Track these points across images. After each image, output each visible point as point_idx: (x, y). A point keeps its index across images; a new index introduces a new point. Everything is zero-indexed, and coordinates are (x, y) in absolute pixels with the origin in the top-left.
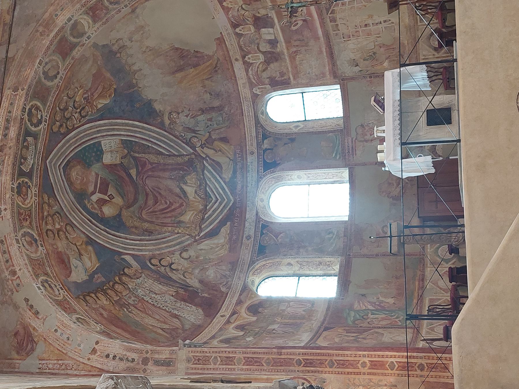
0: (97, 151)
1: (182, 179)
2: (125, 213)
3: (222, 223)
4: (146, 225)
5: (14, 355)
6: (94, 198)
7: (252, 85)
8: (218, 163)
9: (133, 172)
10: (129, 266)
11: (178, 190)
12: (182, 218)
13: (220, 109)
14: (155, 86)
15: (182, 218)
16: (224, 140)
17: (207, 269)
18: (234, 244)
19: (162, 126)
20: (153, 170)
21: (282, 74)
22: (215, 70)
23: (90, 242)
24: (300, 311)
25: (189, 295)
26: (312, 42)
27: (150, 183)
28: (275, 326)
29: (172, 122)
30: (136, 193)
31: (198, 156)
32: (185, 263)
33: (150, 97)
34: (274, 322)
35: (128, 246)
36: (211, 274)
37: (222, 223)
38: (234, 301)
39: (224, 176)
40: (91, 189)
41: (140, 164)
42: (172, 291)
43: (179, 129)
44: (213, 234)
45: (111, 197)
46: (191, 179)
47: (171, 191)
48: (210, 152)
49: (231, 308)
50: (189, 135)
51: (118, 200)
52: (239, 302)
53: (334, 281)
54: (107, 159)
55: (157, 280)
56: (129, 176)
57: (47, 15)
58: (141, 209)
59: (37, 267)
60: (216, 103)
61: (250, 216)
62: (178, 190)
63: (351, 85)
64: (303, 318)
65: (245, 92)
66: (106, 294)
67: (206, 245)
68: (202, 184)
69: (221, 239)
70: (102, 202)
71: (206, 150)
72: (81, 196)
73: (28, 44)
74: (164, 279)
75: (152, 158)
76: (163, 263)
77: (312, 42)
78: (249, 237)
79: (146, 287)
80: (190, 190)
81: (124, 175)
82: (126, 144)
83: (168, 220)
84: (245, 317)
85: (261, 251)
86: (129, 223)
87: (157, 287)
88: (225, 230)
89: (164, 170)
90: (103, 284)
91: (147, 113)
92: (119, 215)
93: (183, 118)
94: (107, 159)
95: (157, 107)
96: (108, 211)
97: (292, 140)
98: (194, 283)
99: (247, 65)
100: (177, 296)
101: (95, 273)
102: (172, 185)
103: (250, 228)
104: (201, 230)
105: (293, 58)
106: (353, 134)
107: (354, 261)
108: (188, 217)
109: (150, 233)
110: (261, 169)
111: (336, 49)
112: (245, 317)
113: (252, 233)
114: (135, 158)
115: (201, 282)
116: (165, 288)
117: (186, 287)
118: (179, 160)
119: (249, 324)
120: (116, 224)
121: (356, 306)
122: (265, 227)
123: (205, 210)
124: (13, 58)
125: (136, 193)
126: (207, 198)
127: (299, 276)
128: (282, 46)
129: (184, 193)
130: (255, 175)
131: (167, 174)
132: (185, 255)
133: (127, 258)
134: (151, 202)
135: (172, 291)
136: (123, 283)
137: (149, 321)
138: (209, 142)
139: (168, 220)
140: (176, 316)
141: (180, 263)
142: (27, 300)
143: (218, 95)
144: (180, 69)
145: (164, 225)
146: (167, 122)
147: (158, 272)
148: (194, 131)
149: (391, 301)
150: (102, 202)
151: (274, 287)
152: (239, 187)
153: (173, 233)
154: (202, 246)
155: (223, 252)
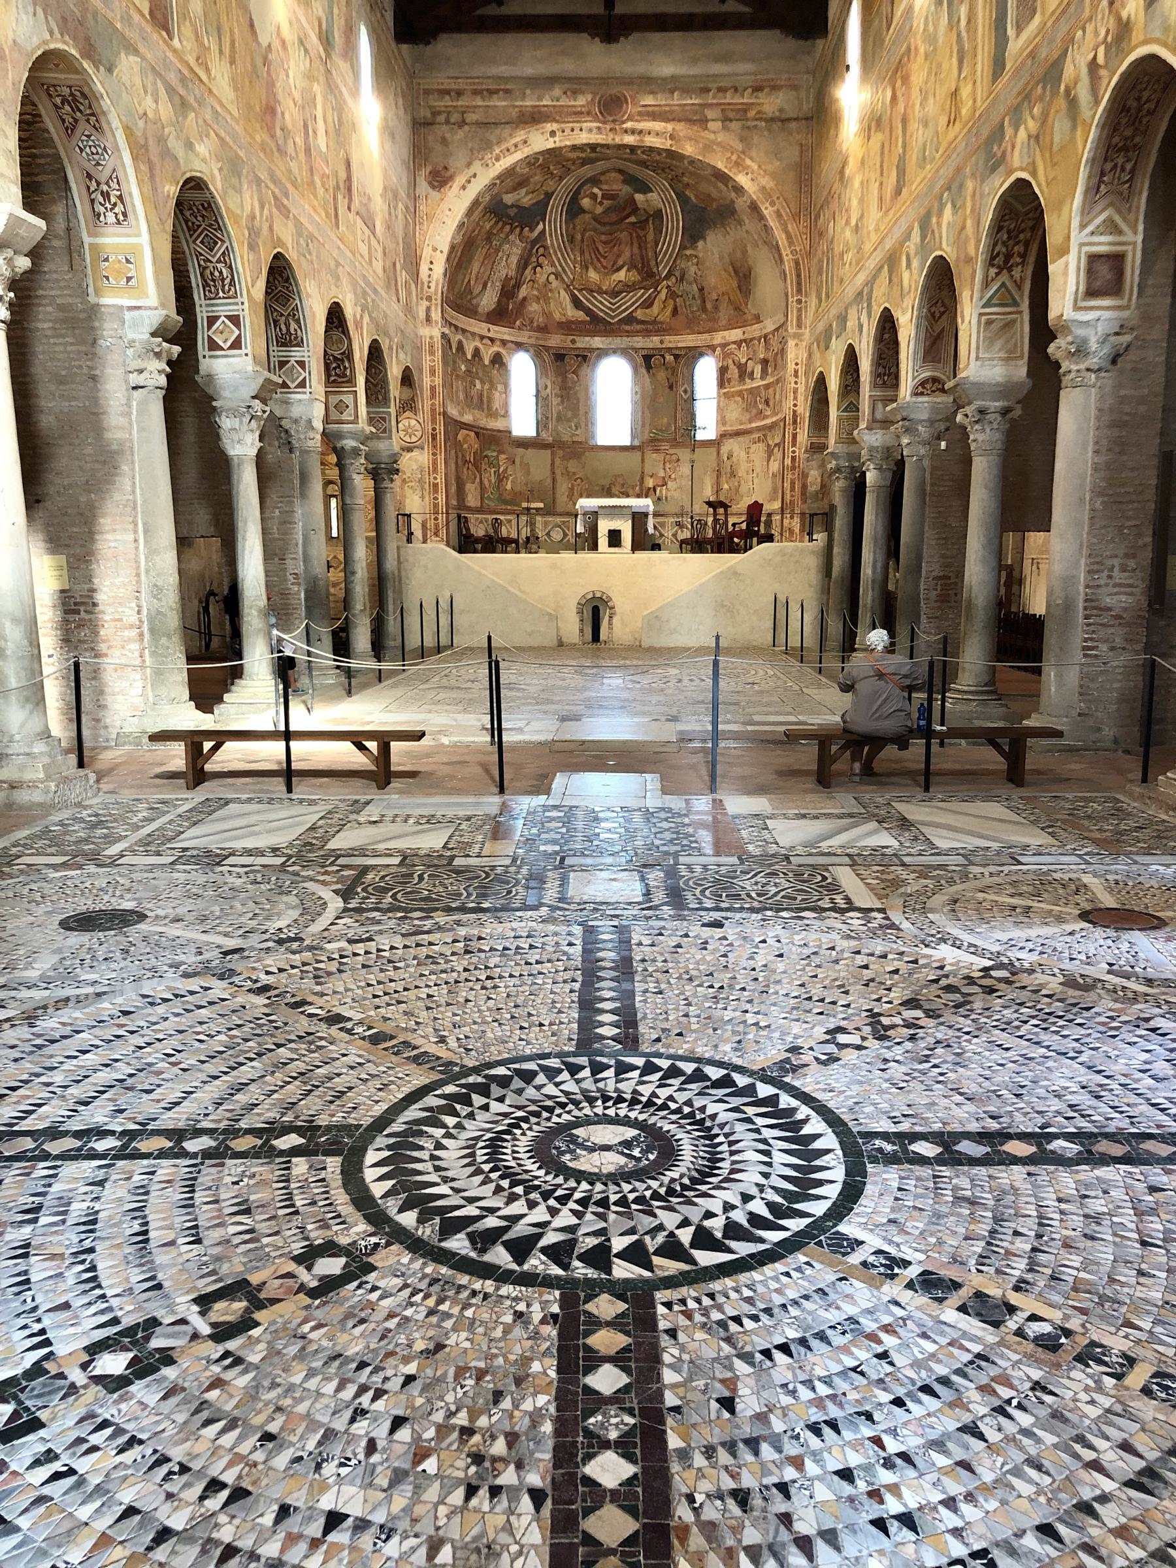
0: (645, 189)
1: (632, 266)
2: (587, 216)
3: (588, 312)
4: (579, 237)
5: (429, 168)
6: (596, 190)
7: (724, 346)
8: (652, 304)
9: (633, 219)
10: (532, 230)
11: (620, 262)
12: (591, 270)
13: (704, 309)
14: (715, 247)
15: (591, 270)
16: (675, 312)
17: (538, 302)
18: (568, 327)
19: (683, 247)
20: (638, 236)
21: (729, 380)
22: (737, 309)
23: (549, 196)
24: (496, 405)
25: (509, 291)
26: (748, 416)
27: (624, 236)
28: (478, 386)
29: (689, 258)
30: (611, 224)
31: (658, 283)
32: (543, 279)
33: (709, 239)
34: (483, 383)
35: (553, 227)
36: (534, 307)
37: (588, 312)
38: (506, 337)
39: (639, 311)
40: (605, 187)
41: (642, 225)
42: (512, 273)
43: (682, 264)
44: (577, 303)
45: (601, 203)
46: (634, 276)
47: (619, 256)
48: (663, 295)
49: (499, 336)
50: (677, 274)
51: (599, 210)
52: (504, 343)
53: (531, 432)
54: (639, 197)
55: (522, 256)
56: (627, 216)
57: (748, 162)
58: (595, 230)
59: (510, 172)
60: (709, 306)
61: (597, 342)
62: (620, 262)
63: (713, 450)
64: (489, 408)
65: (718, 338)
66: (497, 223)
67: (565, 297)
68: (629, 287)
69: (572, 313)
70: (593, 197)
71: (665, 291)
72: (594, 181)
73: (719, 144)
74: (523, 264)
75: (651, 236)
76: (541, 259)
77: (748, 416)
78: (573, 342)
79: (513, 251)
80: (622, 275)
81: (628, 211)
82: (658, 214)
83: (587, 255)
84: (487, 354)
85: (560, 357)
86: (577, 221)
87: (514, 260)
88: (581, 315)
89: (640, 247)
90: (508, 216)
91: (694, 233)
92: (584, 211)
93: (693, 269)
94: (639, 197)
95: (700, 244)
96: (586, 202)
97: (671, 387)
98: (523, 292)
99: (739, 343)
100: (507, 279)
101: (518, 207)
102: (626, 255)
103: (583, 342)
104: (580, 290)
105: (740, 393)
106: (672, 451)
107: (549, 452)
108: (593, 275)
109: (572, 240)
110: (644, 352)
111: (740, 439)
112: (487, 354)
113: (578, 345)
114: (647, 220)
115: (525, 299)
116: (514, 266)
117: (518, 285)
118: (653, 263)
119: (481, 359)
120: (574, 210)
121: (503, 456)
122: (586, 358)
123: (601, 292)
124: (706, 128)
125: (611, 224)
126: (615, 293)
127: (537, 396)
128: (749, 384)
129: (618, 270)
130: (640, 345)
131: (636, 250)
132: (552, 277)
133: (541, 227)
134: (603, 238)
135: (512, 273)
136: (512, 231)
137: (476, 266)
138: (672, 295)
139: (587, 255)
140: (485, 286)
141: (541, 277)
142: (475, 176)
143: (716, 308)
144: (736, 271)
145: (582, 253)
146: (688, 252)
147: (530, 255)
148: (682, 279)
149: (509, 487)
150: (593, 197)
151: (523, 371)
152: (627, 328)
153: (574, 262)
154: (563, 292)
155: (557, 316)
